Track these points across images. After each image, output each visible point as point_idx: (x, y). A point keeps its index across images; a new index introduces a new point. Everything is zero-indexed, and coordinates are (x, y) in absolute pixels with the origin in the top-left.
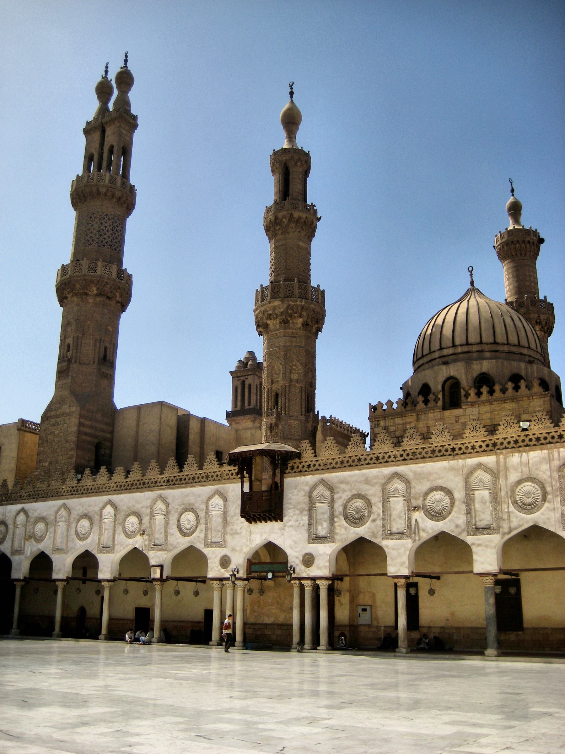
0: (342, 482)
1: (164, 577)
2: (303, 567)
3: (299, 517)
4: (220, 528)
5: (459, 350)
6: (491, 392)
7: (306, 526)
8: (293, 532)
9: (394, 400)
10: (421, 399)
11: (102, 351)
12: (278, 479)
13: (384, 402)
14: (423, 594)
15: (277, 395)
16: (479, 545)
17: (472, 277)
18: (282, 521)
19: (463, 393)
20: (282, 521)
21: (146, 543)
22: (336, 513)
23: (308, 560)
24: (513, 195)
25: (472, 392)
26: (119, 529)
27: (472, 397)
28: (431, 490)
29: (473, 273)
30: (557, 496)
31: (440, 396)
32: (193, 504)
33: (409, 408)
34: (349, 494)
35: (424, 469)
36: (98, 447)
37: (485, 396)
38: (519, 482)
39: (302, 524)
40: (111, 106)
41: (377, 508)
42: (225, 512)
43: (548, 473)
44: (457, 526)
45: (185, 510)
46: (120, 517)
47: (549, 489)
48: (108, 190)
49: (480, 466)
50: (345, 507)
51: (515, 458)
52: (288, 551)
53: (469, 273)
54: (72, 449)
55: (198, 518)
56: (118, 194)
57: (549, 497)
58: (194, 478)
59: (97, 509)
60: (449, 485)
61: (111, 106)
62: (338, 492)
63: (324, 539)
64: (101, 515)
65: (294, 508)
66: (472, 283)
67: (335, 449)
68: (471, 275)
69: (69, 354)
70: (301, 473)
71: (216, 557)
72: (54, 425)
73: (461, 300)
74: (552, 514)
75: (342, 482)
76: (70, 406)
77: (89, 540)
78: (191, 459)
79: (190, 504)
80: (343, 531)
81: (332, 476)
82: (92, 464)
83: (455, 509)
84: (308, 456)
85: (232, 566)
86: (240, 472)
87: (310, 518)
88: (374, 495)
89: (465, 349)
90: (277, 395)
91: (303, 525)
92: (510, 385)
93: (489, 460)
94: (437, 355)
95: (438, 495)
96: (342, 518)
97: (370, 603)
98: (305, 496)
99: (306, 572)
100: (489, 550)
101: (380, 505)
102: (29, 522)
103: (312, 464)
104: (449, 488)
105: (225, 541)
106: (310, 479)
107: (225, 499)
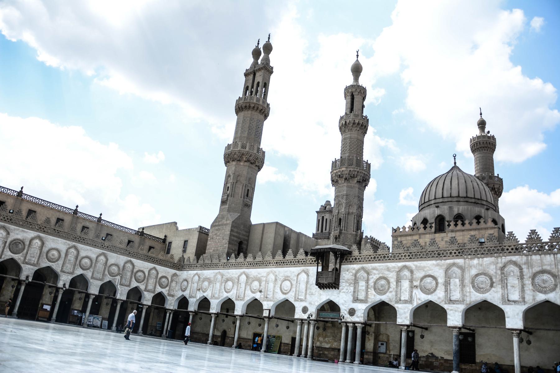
0: (374, 269)
1: (271, 316)
2: (349, 316)
3: (348, 288)
4: (304, 291)
5: (446, 200)
6: (463, 224)
7: (352, 293)
8: (345, 296)
9: (407, 226)
10: (422, 226)
11: (246, 191)
12: (338, 266)
13: (401, 227)
14: (417, 338)
15: (340, 219)
16: (451, 310)
18: (338, 289)
19: (447, 223)
20: (338, 289)
21: (262, 296)
22: (369, 287)
23: (352, 312)
25: (452, 223)
26: (248, 288)
27: (452, 227)
28: (425, 276)
30: (499, 284)
31: (433, 225)
32: (289, 277)
33: (415, 230)
34: (378, 276)
35: (422, 265)
36: (240, 243)
37: (460, 227)
38: (477, 275)
40: (259, 61)
41: (393, 285)
42: (307, 282)
43: (495, 271)
44: (439, 298)
45: (286, 280)
46: (250, 280)
47: (494, 280)
49: (454, 264)
50: (375, 283)
51: (476, 261)
52: (341, 307)
55: (292, 284)
56: (260, 108)
57: (494, 284)
58: (291, 262)
59: (237, 276)
60: (435, 274)
61: (259, 61)
63: (362, 301)
64: (238, 280)
66: (455, 163)
67: (372, 250)
69: (228, 192)
72: (217, 230)
73: (448, 172)
74: (496, 295)
75: (374, 269)
77: (231, 293)
78: (290, 251)
79: (288, 277)
80: (373, 297)
82: (236, 253)
83: (438, 288)
84: (356, 253)
85: (309, 313)
86: (317, 260)
87: (355, 288)
88: (392, 278)
89: (450, 199)
90: (340, 219)
92: (475, 221)
93: (460, 261)
94: (433, 202)
95: (429, 280)
96: (373, 289)
97: (386, 340)
100: (457, 313)
101: (395, 283)
103: (357, 258)
104: (435, 276)
105: (306, 298)
106: (356, 266)
107: (308, 275)
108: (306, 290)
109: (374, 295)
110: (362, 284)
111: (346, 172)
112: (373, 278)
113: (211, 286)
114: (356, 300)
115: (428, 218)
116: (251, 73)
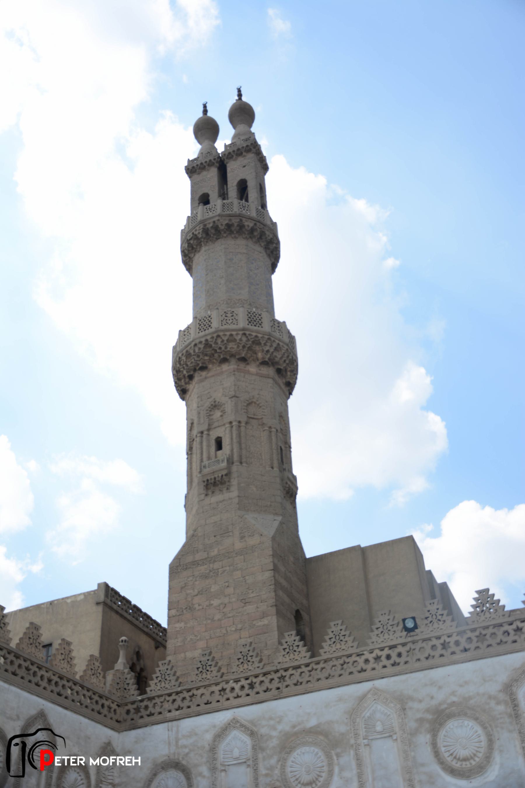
48: (255, 224)
54: (264, 615)
59: (493, 688)
72: (205, 577)
76: (242, 538)
102: (263, 749)
113: (348, 759)
116: (210, 164)
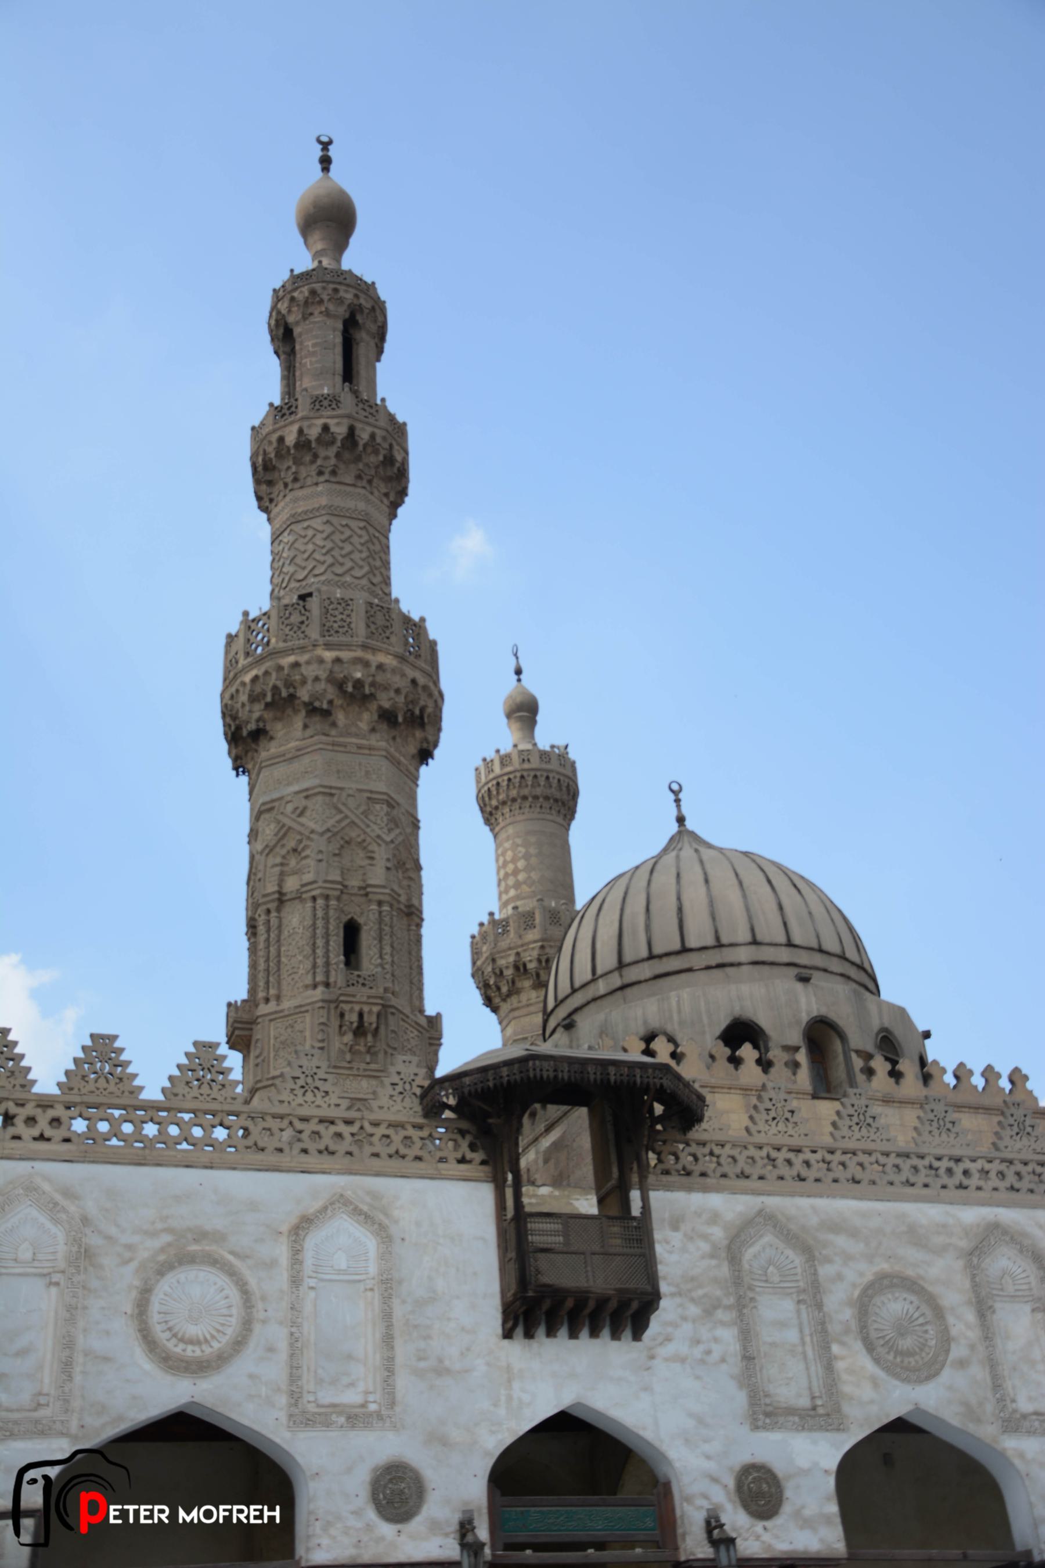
0: (836, 1226)
17: (678, 806)
19: (858, 1063)
22: (834, 1328)
24: (519, 680)
25: (880, 1065)
27: (882, 1079)
29: (681, 796)
31: (802, 1057)
32: (220, 1237)
34: (869, 1272)
39: (716, 1356)
41: (963, 1323)
45: (186, 1259)
53: (672, 797)
62: (828, 1260)
65: (680, 1294)
66: (681, 820)
68: (677, 801)
70: (689, 1177)
71: (349, 1470)
79: (201, 1235)
80: (866, 1392)
81: (805, 1208)
87: (746, 1335)
89: (818, 960)
91: (723, 1360)
94: (743, 954)
96: (858, 1345)
98: (712, 1256)
99: (758, 1538)
101: (971, 1317)
108: (388, 1340)
109: (875, 1382)
110: (778, 1314)
111: (397, 681)
112: (845, 1279)
114: (764, 1413)
115: (764, 1020)
